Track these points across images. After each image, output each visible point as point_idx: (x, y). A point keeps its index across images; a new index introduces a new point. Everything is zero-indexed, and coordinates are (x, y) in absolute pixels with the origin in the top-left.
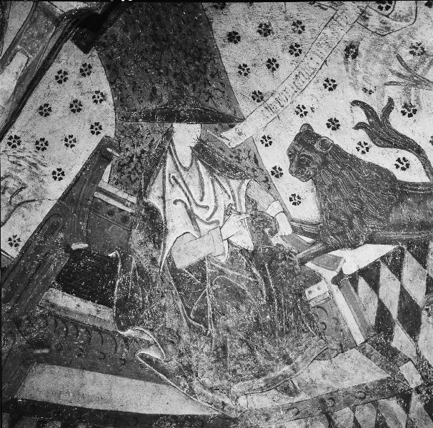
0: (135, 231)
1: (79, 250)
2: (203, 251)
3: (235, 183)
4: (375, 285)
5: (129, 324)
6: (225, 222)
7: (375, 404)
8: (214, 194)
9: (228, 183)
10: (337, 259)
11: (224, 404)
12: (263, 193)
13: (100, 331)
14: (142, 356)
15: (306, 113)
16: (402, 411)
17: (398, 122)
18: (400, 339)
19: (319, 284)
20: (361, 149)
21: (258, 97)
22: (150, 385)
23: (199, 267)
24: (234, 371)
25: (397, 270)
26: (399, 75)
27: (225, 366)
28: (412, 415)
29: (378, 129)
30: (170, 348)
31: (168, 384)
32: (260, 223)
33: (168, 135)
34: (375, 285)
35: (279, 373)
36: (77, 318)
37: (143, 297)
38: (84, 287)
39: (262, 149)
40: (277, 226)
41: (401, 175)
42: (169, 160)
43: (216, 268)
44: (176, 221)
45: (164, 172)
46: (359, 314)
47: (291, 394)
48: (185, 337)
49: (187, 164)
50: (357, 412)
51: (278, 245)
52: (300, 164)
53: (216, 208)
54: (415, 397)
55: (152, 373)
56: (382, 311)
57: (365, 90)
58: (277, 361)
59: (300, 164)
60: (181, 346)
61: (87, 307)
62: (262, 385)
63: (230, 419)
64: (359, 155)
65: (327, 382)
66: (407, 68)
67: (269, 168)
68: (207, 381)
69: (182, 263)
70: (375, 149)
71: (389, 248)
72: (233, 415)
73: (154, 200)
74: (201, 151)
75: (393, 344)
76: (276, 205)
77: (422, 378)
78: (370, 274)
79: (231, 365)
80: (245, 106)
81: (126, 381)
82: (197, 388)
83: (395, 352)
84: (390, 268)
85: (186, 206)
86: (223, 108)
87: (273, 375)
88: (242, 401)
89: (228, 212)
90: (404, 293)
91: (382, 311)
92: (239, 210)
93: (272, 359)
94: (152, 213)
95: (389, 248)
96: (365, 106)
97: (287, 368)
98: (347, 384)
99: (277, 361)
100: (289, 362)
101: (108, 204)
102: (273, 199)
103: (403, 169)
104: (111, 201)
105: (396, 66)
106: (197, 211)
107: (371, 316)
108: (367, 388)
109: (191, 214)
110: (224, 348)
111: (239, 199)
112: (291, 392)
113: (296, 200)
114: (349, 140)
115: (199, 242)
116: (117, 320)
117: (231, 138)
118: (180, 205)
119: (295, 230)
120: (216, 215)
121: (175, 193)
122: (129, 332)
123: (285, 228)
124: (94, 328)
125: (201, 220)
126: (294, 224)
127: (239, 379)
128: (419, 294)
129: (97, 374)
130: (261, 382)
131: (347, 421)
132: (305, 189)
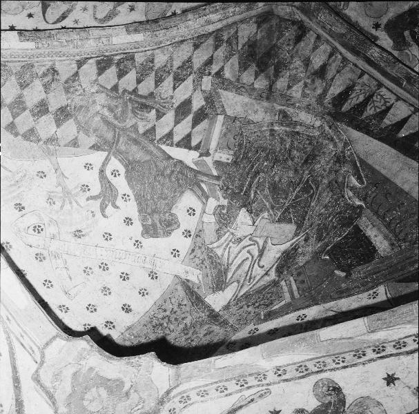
0: (301, 264)
1: (343, 271)
3: (219, 252)
4: (189, 137)
5: (354, 208)
6: (245, 237)
7: (238, 80)
8: (235, 255)
9: (223, 255)
10: (196, 163)
11: (330, 127)
12: (207, 232)
13: (376, 213)
14: (362, 183)
15: (137, 241)
16: (226, 68)
17: (96, 189)
18: (198, 103)
19: (219, 159)
20: (127, 198)
21: (153, 275)
22: (370, 162)
24: (310, 144)
25: (170, 135)
26: (71, 203)
27: (313, 150)
28: (222, 64)
29: (108, 195)
30: (340, 179)
31: (358, 157)
32: (225, 219)
33: (227, 307)
34: (189, 137)
35: (283, 128)
36: (383, 229)
37: (332, 220)
38: (362, 246)
39: (183, 253)
40: (216, 209)
41: (122, 170)
42: (242, 293)
43: (273, 211)
44: (273, 254)
45: (251, 288)
46: (209, 131)
47: (285, 112)
48: (325, 181)
49: (236, 284)
50: (251, 82)
51: (225, 198)
52: (169, 225)
53: (244, 248)
54: (213, 72)
55: (363, 168)
56: (196, 122)
57: (94, 216)
58: (279, 135)
60: (332, 176)
61: (371, 233)
62: (298, 127)
63: (332, 117)
64: (132, 197)
65: (257, 107)
66: (64, 201)
67: (189, 240)
68: (331, 147)
69: (290, 228)
70: (121, 192)
71: (164, 147)
72: (328, 118)
73: (273, 275)
75: (204, 103)
76: (205, 219)
77: (202, 78)
78: (186, 143)
79: (309, 149)
80: (166, 281)
81: (383, 172)
82: (340, 145)
83: (206, 99)
84: (172, 138)
85: (259, 260)
86: (181, 292)
87: (288, 129)
88: (318, 123)
89: (240, 240)
90: (177, 122)
91: (196, 122)
92: (232, 236)
93: (281, 138)
94: (279, 271)
95: (164, 147)
96: (103, 209)
97: (276, 128)
98: (246, 99)
99: (279, 135)
100: (272, 130)
101: (298, 288)
102: (204, 224)
103: (118, 171)
104: (294, 287)
105: (67, 207)
106: (256, 253)
107: (204, 124)
108: (236, 91)
109: (261, 255)
110: (306, 161)
111: (225, 241)
112: (285, 115)
113: (191, 212)
114: (130, 208)
115: (273, 234)
116: (359, 215)
117: (195, 276)
118: (262, 263)
119: (207, 198)
120: (247, 244)
121: (258, 272)
122: (358, 203)
123: (212, 203)
124: (378, 216)
125: (258, 247)
126: (205, 202)
127: (310, 138)
128: (170, 116)
129: (400, 185)
130: (298, 129)
131: (261, 80)
132: (180, 210)
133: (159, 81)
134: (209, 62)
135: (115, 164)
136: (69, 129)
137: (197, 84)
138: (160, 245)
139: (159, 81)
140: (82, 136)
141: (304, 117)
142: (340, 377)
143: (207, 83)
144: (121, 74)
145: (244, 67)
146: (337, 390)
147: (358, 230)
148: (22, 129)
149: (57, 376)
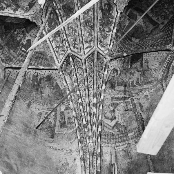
2: (15, 36)
23: (13, 37)
25: (25, 53)
32: (21, 40)
44: (16, 33)
59: (27, 41)
73: (17, 30)
74: (23, 31)
78: (23, 51)
90: (23, 54)
113: (25, 42)
121: (18, 31)
123: (22, 42)
132: (26, 42)
134: (16, 61)
136: (37, 55)
137: (19, 58)
138: (30, 38)
141: (6, 49)
142: (13, 13)
143: (18, 58)
145: (12, 59)
146: (14, 12)
147: (5, 31)
148: (42, 55)
149: (40, 21)
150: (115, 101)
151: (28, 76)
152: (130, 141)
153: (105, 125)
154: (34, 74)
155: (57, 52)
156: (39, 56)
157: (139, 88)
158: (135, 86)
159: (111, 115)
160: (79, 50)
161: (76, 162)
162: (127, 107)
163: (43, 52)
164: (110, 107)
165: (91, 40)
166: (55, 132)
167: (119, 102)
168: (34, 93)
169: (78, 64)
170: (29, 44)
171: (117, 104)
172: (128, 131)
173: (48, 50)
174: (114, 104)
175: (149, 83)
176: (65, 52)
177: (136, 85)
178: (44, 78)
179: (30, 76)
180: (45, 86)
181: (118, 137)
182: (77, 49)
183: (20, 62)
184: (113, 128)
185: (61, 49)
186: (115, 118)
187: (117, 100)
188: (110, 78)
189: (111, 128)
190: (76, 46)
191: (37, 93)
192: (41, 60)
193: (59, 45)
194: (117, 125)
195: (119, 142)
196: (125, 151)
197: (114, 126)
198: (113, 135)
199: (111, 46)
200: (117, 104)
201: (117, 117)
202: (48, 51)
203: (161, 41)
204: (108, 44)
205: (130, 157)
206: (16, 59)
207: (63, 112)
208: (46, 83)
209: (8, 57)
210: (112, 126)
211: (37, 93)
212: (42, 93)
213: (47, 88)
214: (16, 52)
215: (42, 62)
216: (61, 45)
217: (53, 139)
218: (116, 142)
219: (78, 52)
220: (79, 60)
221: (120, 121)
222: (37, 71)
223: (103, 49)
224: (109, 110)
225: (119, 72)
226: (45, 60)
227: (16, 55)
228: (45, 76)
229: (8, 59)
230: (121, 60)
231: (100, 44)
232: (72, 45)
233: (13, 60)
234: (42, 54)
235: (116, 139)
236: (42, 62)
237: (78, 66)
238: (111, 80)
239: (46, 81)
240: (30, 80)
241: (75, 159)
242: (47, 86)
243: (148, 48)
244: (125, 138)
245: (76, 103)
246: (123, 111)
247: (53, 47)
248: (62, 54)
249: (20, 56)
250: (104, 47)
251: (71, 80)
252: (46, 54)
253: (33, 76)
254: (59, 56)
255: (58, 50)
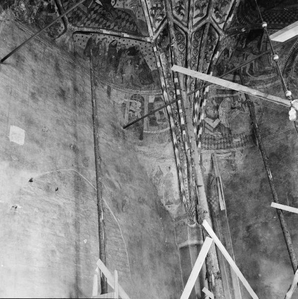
41: (111, 3)
90: (98, 10)
128: (99, 11)
133: (99, 20)
134: (87, 21)
135: (113, 4)
136: (120, 13)
137: (91, 16)
139: (99, 20)
140: (117, 12)
143: (89, 16)
144: (106, 24)
145: (81, 17)
148: (128, 16)
150: (220, 94)
151: (103, 45)
152: (235, 149)
153: (206, 125)
154: (112, 42)
155: (153, 15)
156: (123, 16)
157: (252, 78)
158: (247, 75)
159: (214, 112)
160: (186, 19)
161: (171, 171)
162: (235, 104)
163: (130, 11)
164: (214, 102)
165: (204, 5)
166: (144, 131)
167: (225, 96)
168: (112, 73)
169: (179, 38)
170: (288, 175)
171: (222, 99)
172: (233, 135)
173: (139, 10)
174: (218, 98)
175: (265, 73)
176: (163, 17)
177: (248, 74)
178: (126, 49)
179: (105, 45)
180: (126, 62)
181: (221, 142)
182: (182, 16)
183: (92, 22)
184: (215, 129)
185: (158, 11)
186: (218, 117)
187: (223, 93)
188: (219, 62)
189: (212, 130)
190: (182, 11)
191: (116, 72)
192: (125, 22)
193: (157, 5)
194: (219, 126)
195: (221, 148)
196: (228, 160)
197: (216, 127)
198: (214, 139)
199: (230, 19)
200: (222, 99)
201: (220, 116)
202: (139, 12)
203: (292, 16)
204: (226, 15)
205: (234, 169)
206: (87, 17)
207: (152, 104)
208: (129, 57)
209: (75, 13)
210: (214, 127)
211: (116, 72)
212: (122, 72)
213: (129, 65)
214: (87, 6)
215: (125, 26)
216: (159, 6)
217: (142, 141)
218: (217, 149)
219: (183, 20)
220: (183, 33)
221: (223, 120)
222: (117, 39)
223: (218, 20)
224: (212, 106)
225: (230, 54)
226: (130, 24)
227: (86, 11)
228: (127, 47)
229: (75, 18)
230: (235, 37)
231: (215, 12)
232: (176, 8)
233: (83, 19)
234: (127, 14)
235: (218, 144)
236: (125, 26)
237: (179, 41)
238: (219, 64)
239: (129, 54)
240: (105, 51)
241: (169, 168)
242: (129, 62)
243: (273, 23)
244: (229, 145)
245: (171, 93)
246: (228, 108)
247: (147, 8)
248: (159, 20)
249: (93, 12)
250: (220, 17)
251: (168, 59)
252: (135, 16)
253: (110, 46)
254: (154, 22)
255: (153, 13)
